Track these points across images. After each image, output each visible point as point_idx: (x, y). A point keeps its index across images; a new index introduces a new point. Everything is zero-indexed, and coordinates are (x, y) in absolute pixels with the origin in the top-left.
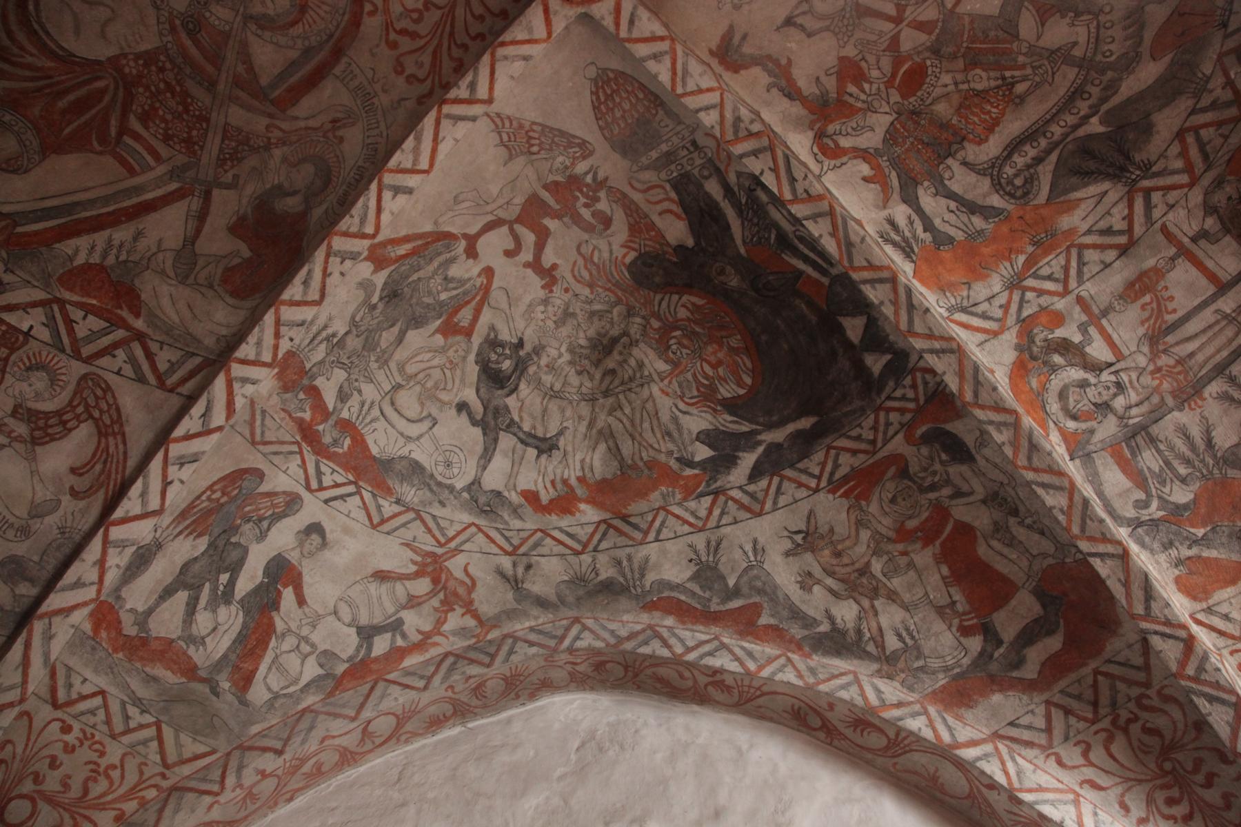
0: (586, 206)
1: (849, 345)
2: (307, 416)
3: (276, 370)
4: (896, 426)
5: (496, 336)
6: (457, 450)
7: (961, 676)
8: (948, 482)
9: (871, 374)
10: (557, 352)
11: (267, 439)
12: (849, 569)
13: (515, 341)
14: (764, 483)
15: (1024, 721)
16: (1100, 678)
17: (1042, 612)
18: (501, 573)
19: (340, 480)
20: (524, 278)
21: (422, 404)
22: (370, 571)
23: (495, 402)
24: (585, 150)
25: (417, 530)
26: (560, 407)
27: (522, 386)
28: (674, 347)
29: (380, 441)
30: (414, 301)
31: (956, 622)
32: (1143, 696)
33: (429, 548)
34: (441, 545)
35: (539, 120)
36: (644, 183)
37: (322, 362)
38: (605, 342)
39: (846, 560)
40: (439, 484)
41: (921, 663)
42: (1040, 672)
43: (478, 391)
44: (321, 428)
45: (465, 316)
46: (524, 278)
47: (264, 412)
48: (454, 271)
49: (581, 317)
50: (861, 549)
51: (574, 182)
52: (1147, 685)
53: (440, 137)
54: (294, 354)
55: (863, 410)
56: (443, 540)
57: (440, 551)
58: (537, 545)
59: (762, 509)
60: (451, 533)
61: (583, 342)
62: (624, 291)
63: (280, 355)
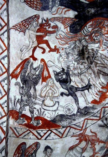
0: (49, 28)
2: (26, 122)
3: (11, 117)
5: (56, 72)
6: (69, 105)
10: (73, 64)
11: (20, 134)
13: (61, 70)
18: (101, 126)
19: (45, 132)
20: (51, 55)
21: (52, 100)
22: (68, 149)
23: (69, 87)
24: (37, 17)
25: (72, 131)
26: (84, 76)
27: (72, 78)
28: (96, 38)
29: (48, 116)
30: (31, 79)
33: (78, 133)
34: (81, 130)
35: (23, 20)
36: (55, 11)
37: (21, 108)
38: (81, 52)
40: (70, 116)
43: (63, 88)
44: (31, 123)
45: (46, 73)
46: (51, 55)
47: (15, 128)
48: (35, 66)
49: (71, 52)
51: (41, 25)
53: (3, 40)
54: (12, 110)
56: (80, 129)
57: (82, 132)
58: (104, 113)
60: (81, 126)
61: (76, 57)
62: (75, 37)
63: (6, 112)
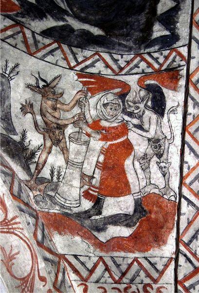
1: (154, 10)
4: (140, 70)
7: (67, 215)
8: (140, 117)
9: (152, 35)
12: (54, 120)
14: (47, 41)
15: (82, 259)
16: (135, 263)
17: (131, 213)
31: (86, 187)
32: (149, 285)
39: (56, 114)
41: (53, 194)
42: (108, 241)
50: (69, 115)
52: (155, 281)
55: (130, 49)
59: (35, 53)
